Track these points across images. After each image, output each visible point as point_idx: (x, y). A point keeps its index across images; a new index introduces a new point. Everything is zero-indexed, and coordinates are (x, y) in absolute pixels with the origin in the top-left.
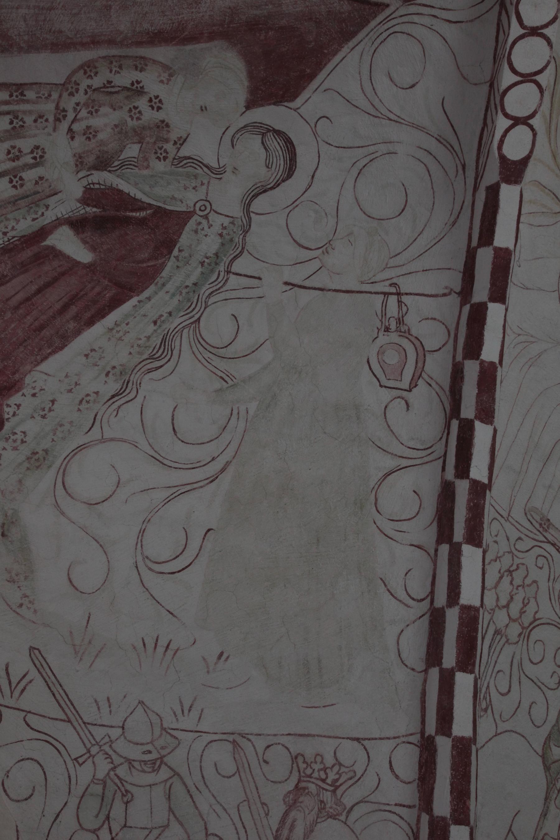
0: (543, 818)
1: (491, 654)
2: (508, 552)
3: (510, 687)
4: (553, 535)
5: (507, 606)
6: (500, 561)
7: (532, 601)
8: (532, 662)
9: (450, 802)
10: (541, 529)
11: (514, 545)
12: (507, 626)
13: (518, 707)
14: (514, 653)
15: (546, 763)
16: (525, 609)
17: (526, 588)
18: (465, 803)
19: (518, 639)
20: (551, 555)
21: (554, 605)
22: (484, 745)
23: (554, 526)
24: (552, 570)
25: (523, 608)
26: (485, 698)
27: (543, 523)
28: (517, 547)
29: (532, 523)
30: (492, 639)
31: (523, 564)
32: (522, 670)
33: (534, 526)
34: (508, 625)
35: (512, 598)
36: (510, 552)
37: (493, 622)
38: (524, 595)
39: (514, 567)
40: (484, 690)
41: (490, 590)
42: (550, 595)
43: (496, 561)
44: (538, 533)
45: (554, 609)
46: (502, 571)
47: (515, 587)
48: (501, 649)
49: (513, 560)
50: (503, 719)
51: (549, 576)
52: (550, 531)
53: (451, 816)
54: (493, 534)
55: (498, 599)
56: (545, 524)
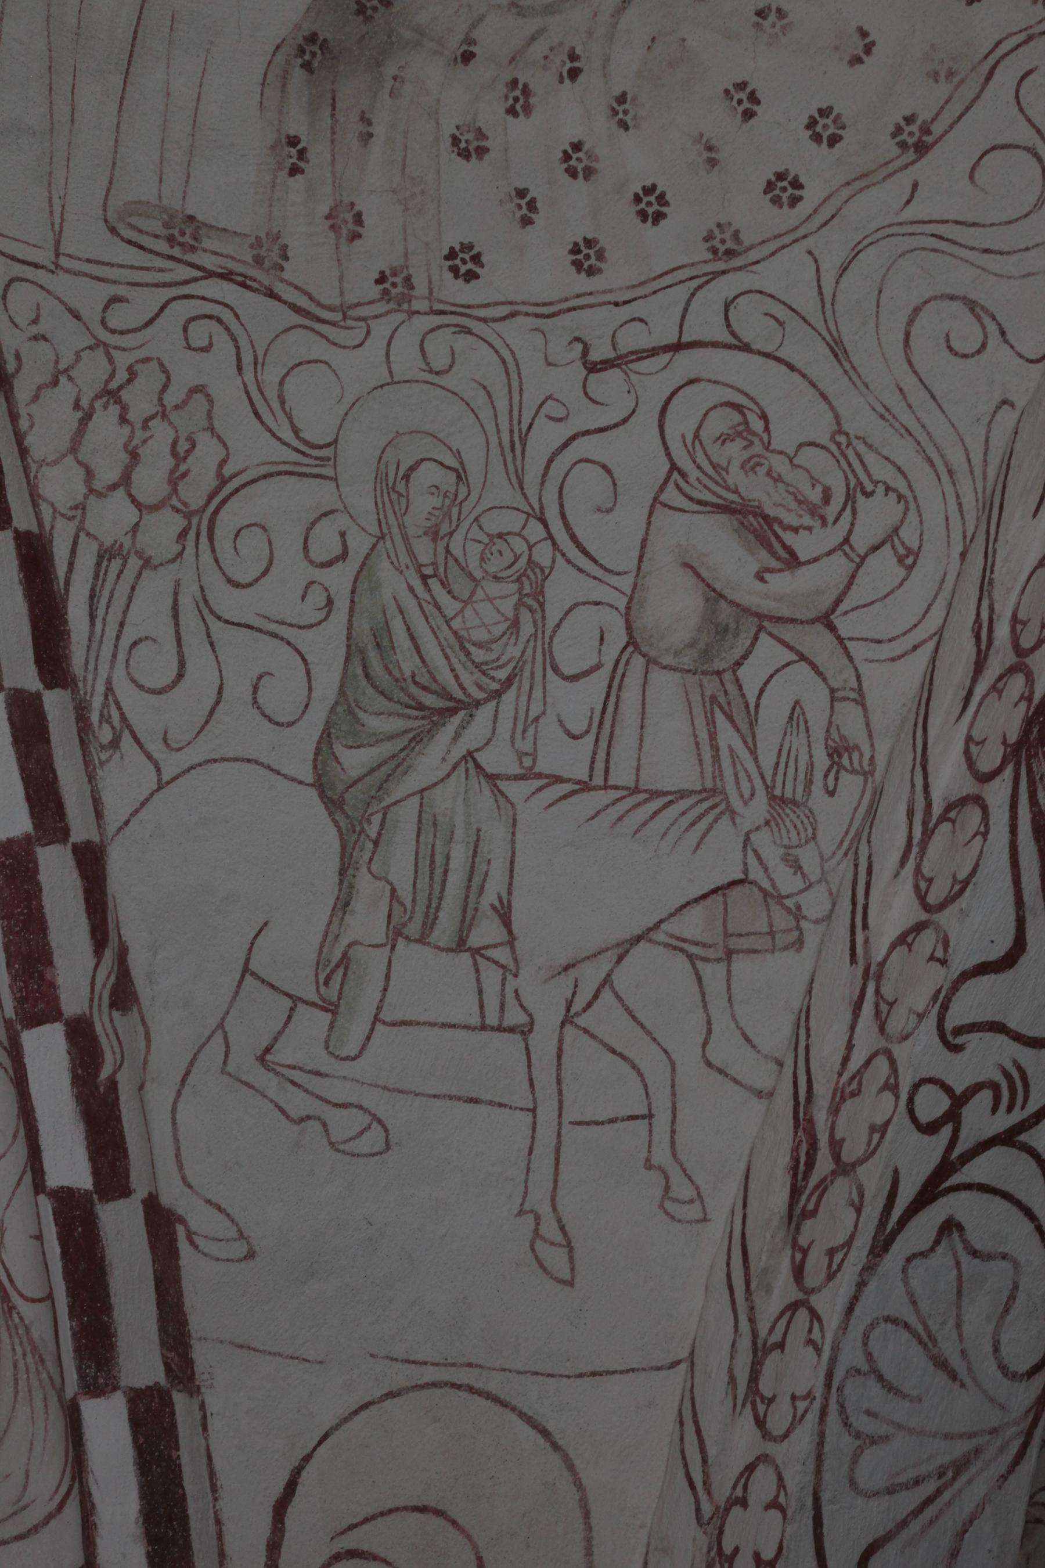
0: (340, 914)
1: (101, 612)
2: (90, 348)
3: (182, 664)
4: (215, 253)
5: (125, 480)
6: (70, 379)
7: (204, 440)
8: (237, 585)
9: (10, 986)
10: (176, 252)
11: (103, 323)
12: (135, 528)
13: (218, 703)
14: (178, 583)
15: (330, 793)
16: (183, 468)
17: (173, 417)
18: (42, 977)
19: (180, 547)
20: (226, 305)
21: (274, 427)
22: (127, 823)
23: (211, 227)
24: (243, 342)
25: (177, 466)
26: (105, 719)
27: (176, 232)
28: (112, 324)
29: (141, 247)
30: (96, 576)
31: (146, 360)
32: (212, 612)
33: (151, 251)
34: (137, 524)
35: (134, 456)
36: (99, 344)
37: (88, 534)
38: (172, 434)
39: (122, 376)
40: (97, 702)
41: (55, 462)
42: (252, 404)
43: (55, 383)
44: (170, 264)
45: (274, 435)
46: (85, 403)
47: (138, 426)
48: (133, 589)
49: (111, 360)
50: (174, 745)
51: (239, 360)
52: (206, 243)
53: (16, 1014)
54: (22, 322)
55: (89, 473)
56: (183, 233)
